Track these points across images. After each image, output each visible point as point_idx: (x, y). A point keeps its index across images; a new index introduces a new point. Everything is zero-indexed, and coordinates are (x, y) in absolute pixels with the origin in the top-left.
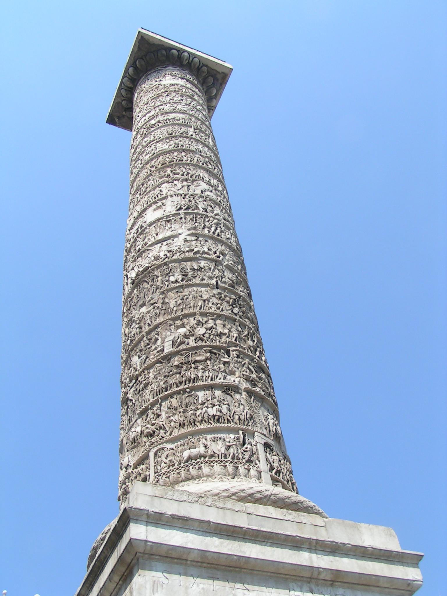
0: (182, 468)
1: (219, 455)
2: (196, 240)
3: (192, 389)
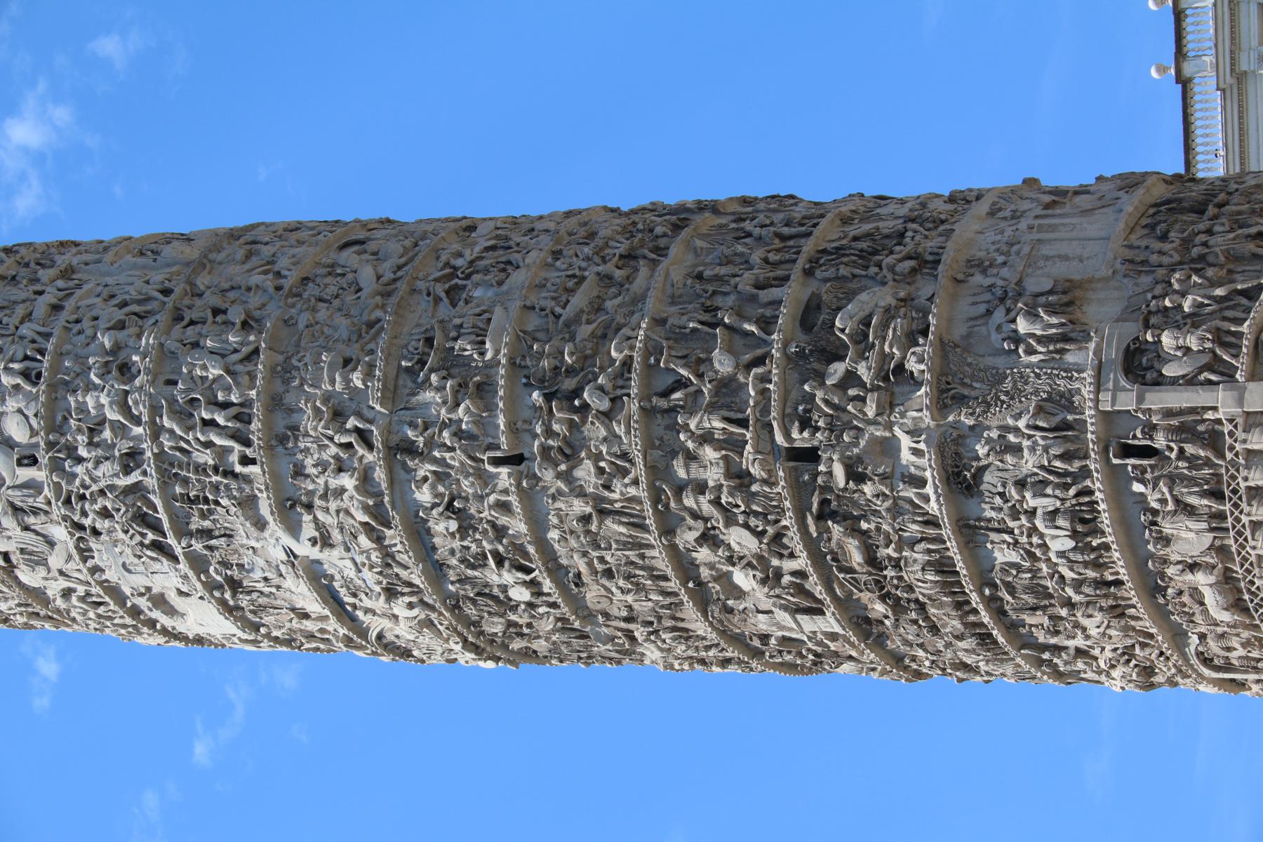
2: (309, 507)
3: (984, 579)
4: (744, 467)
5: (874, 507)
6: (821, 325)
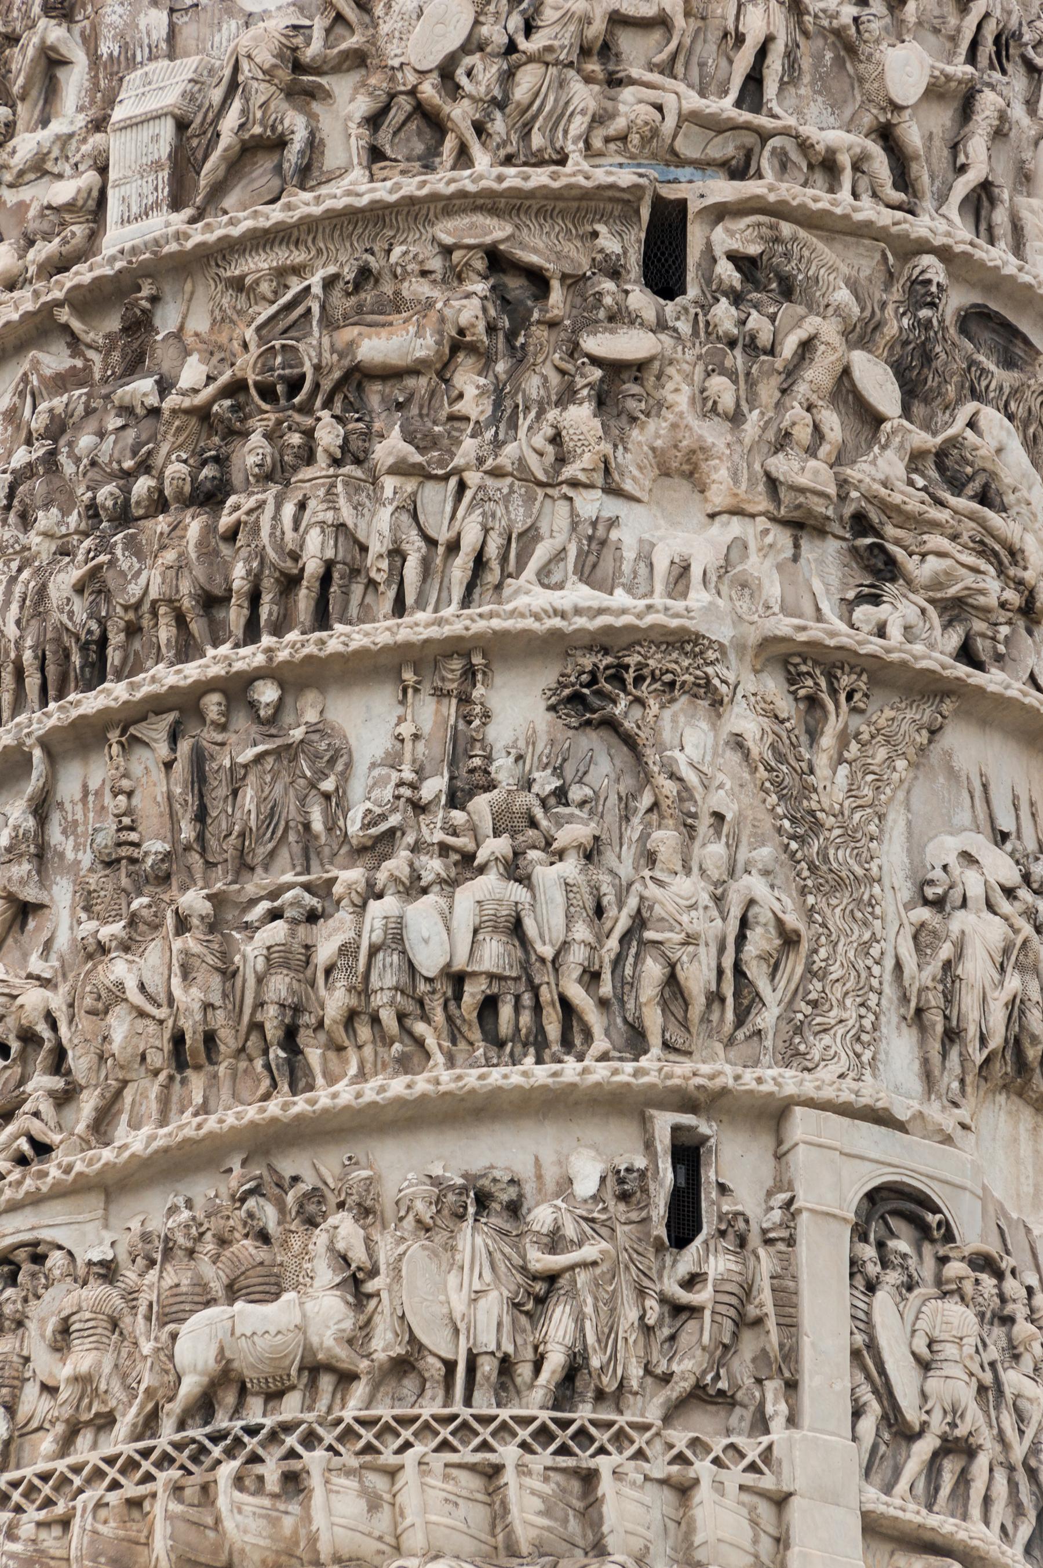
0: (159, 1465)
1: (450, 1366)
5: (524, 424)
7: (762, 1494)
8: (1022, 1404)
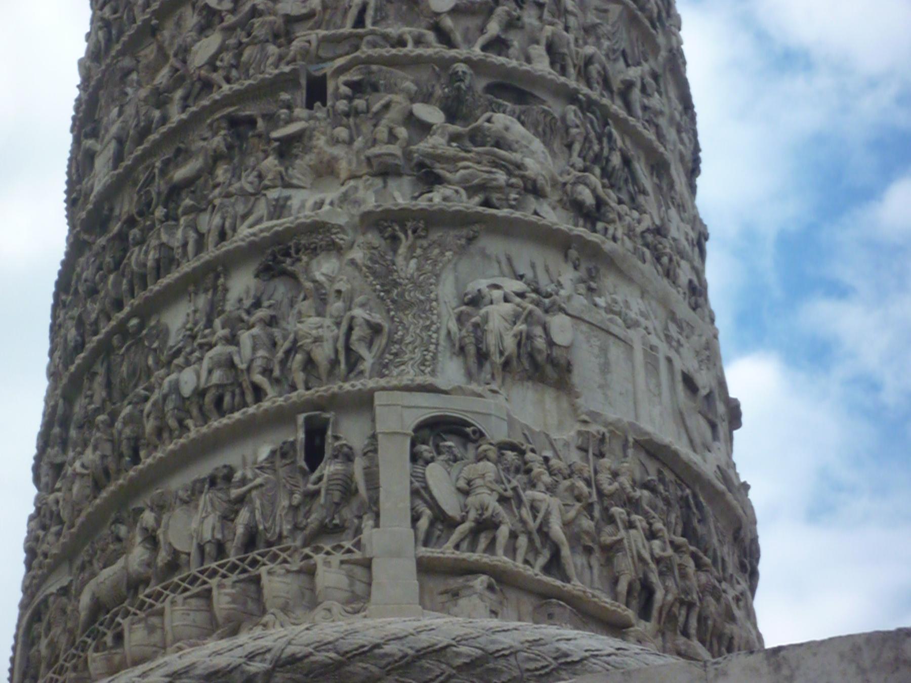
4: (298, 34)
6: (496, 103)
7: (356, 563)
8: (537, 504)
